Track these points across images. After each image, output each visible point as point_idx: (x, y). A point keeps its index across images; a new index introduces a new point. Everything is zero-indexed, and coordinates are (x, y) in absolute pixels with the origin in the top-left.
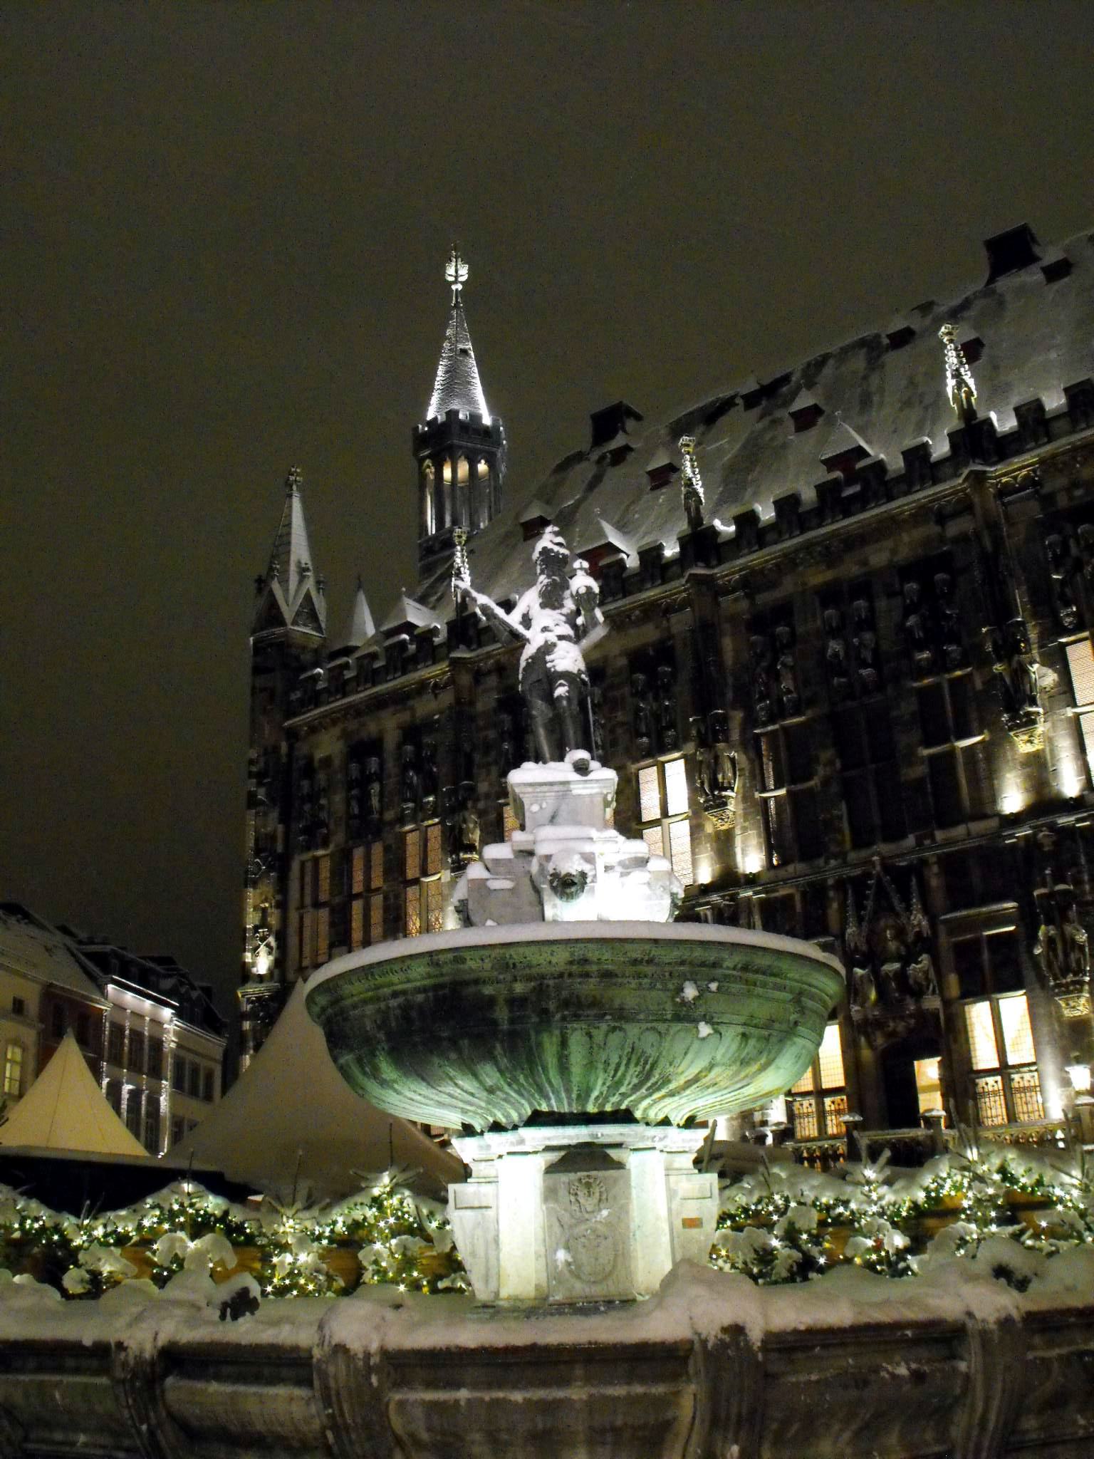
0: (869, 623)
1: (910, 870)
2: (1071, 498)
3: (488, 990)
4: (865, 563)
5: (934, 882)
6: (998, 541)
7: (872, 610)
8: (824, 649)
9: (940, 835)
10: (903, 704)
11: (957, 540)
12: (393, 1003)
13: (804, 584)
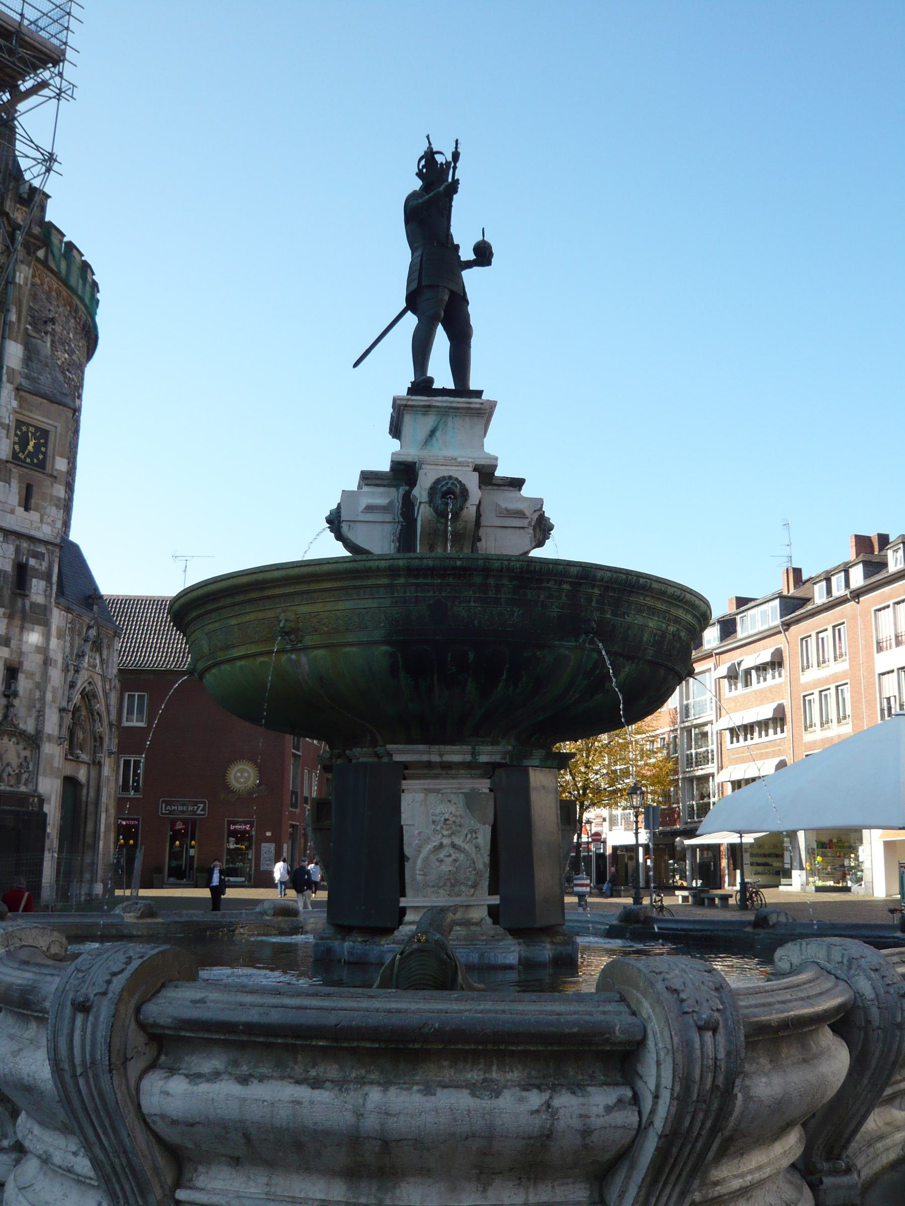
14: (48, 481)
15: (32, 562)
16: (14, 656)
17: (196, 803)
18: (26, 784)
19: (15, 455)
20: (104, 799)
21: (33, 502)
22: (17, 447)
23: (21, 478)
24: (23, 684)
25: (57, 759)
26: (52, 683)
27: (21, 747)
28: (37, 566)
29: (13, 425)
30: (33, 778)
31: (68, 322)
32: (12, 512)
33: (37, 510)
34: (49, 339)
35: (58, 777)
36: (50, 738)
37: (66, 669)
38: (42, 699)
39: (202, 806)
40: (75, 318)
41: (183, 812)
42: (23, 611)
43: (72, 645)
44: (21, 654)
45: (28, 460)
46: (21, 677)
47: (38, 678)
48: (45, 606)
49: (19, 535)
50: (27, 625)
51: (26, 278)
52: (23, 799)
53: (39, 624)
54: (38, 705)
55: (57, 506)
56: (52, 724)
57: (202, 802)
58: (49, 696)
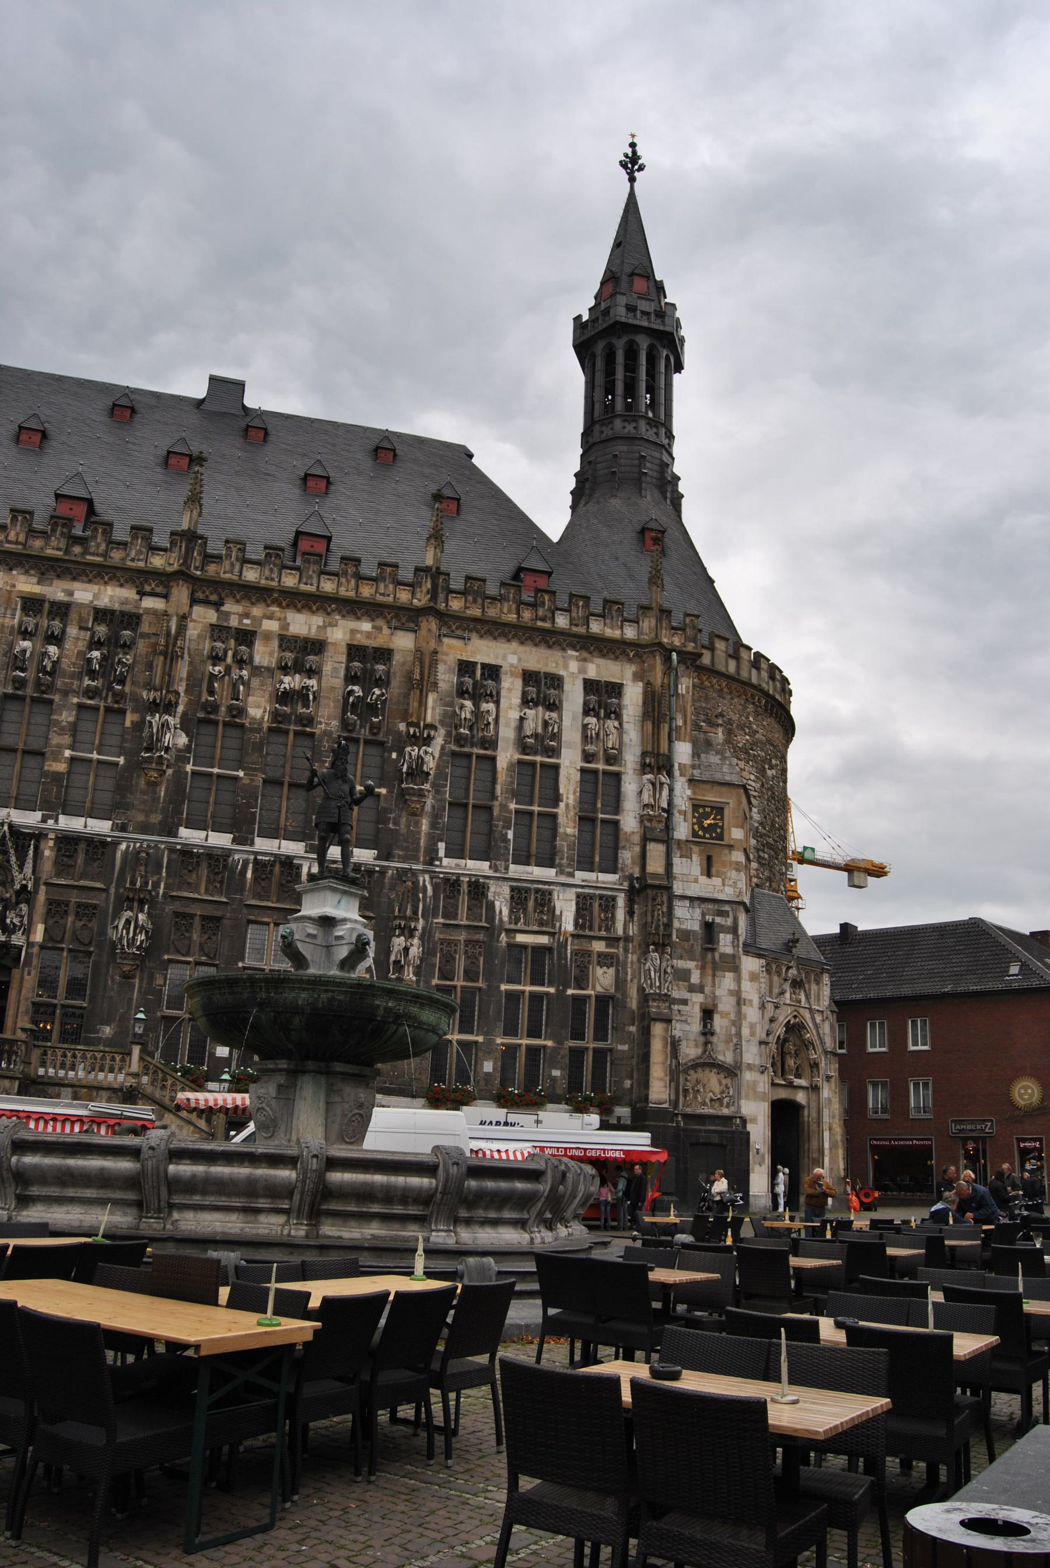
0: (56, 639)
1: (31, 836)
2: (240, 622)
3: (377, 1002)
4: (71, 594)
5: (47, 853)
6: (182, 629)
7: (64, 632)
8: (11, 646)
9: (61, 817)
10: (64, 713)
11: (148, 611)
12: (324, 996)
13: (14, 586)
14: (726, 851)
15: (718, 920)
16: (709, 1000)
17: (984, 1121)
18: (728, 1106)
19: (695, 834)
20: (826, 1118)
21: (714, 870)
22: (696, 827)
23: (701, 853)
24: (719, 1023)
25: (762, 1084)
26: (748, 1020)
27: (722, 1076)
28: (723, 923)
29: (690, 811)
30: (735, 1100)
31: (745, 708)
32: (696, 881)
33: (718, 876)
34: (720, 730)
35: (764, 1101)
36: (750, 1067)
37: (763, 1007)
38: (739, 1035)
39: (989, 1124)
40: (753, 703)
41: (971, 1130)
42: (714, 961)
43: (771, 987)
44: (715, 997)
45: (707, 836)
46: (717, 1017)
47: (733, 1017)
48: (734, 956)
49: (702, 900)
50: (719, 973)
51: (687, 688)
52: (728, 1119)
53: (729, 971)
54: (735, 1040)
55: (738, 870)
56: (752, 1054)
57: (991, 1121)
58: (745, 1031)
